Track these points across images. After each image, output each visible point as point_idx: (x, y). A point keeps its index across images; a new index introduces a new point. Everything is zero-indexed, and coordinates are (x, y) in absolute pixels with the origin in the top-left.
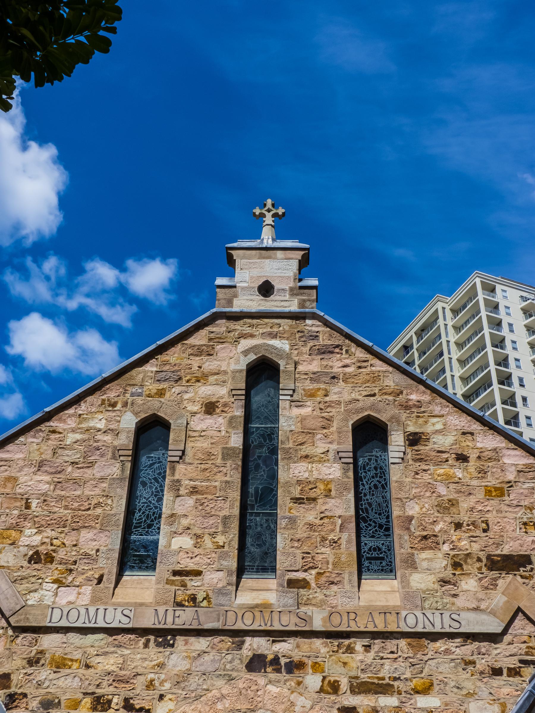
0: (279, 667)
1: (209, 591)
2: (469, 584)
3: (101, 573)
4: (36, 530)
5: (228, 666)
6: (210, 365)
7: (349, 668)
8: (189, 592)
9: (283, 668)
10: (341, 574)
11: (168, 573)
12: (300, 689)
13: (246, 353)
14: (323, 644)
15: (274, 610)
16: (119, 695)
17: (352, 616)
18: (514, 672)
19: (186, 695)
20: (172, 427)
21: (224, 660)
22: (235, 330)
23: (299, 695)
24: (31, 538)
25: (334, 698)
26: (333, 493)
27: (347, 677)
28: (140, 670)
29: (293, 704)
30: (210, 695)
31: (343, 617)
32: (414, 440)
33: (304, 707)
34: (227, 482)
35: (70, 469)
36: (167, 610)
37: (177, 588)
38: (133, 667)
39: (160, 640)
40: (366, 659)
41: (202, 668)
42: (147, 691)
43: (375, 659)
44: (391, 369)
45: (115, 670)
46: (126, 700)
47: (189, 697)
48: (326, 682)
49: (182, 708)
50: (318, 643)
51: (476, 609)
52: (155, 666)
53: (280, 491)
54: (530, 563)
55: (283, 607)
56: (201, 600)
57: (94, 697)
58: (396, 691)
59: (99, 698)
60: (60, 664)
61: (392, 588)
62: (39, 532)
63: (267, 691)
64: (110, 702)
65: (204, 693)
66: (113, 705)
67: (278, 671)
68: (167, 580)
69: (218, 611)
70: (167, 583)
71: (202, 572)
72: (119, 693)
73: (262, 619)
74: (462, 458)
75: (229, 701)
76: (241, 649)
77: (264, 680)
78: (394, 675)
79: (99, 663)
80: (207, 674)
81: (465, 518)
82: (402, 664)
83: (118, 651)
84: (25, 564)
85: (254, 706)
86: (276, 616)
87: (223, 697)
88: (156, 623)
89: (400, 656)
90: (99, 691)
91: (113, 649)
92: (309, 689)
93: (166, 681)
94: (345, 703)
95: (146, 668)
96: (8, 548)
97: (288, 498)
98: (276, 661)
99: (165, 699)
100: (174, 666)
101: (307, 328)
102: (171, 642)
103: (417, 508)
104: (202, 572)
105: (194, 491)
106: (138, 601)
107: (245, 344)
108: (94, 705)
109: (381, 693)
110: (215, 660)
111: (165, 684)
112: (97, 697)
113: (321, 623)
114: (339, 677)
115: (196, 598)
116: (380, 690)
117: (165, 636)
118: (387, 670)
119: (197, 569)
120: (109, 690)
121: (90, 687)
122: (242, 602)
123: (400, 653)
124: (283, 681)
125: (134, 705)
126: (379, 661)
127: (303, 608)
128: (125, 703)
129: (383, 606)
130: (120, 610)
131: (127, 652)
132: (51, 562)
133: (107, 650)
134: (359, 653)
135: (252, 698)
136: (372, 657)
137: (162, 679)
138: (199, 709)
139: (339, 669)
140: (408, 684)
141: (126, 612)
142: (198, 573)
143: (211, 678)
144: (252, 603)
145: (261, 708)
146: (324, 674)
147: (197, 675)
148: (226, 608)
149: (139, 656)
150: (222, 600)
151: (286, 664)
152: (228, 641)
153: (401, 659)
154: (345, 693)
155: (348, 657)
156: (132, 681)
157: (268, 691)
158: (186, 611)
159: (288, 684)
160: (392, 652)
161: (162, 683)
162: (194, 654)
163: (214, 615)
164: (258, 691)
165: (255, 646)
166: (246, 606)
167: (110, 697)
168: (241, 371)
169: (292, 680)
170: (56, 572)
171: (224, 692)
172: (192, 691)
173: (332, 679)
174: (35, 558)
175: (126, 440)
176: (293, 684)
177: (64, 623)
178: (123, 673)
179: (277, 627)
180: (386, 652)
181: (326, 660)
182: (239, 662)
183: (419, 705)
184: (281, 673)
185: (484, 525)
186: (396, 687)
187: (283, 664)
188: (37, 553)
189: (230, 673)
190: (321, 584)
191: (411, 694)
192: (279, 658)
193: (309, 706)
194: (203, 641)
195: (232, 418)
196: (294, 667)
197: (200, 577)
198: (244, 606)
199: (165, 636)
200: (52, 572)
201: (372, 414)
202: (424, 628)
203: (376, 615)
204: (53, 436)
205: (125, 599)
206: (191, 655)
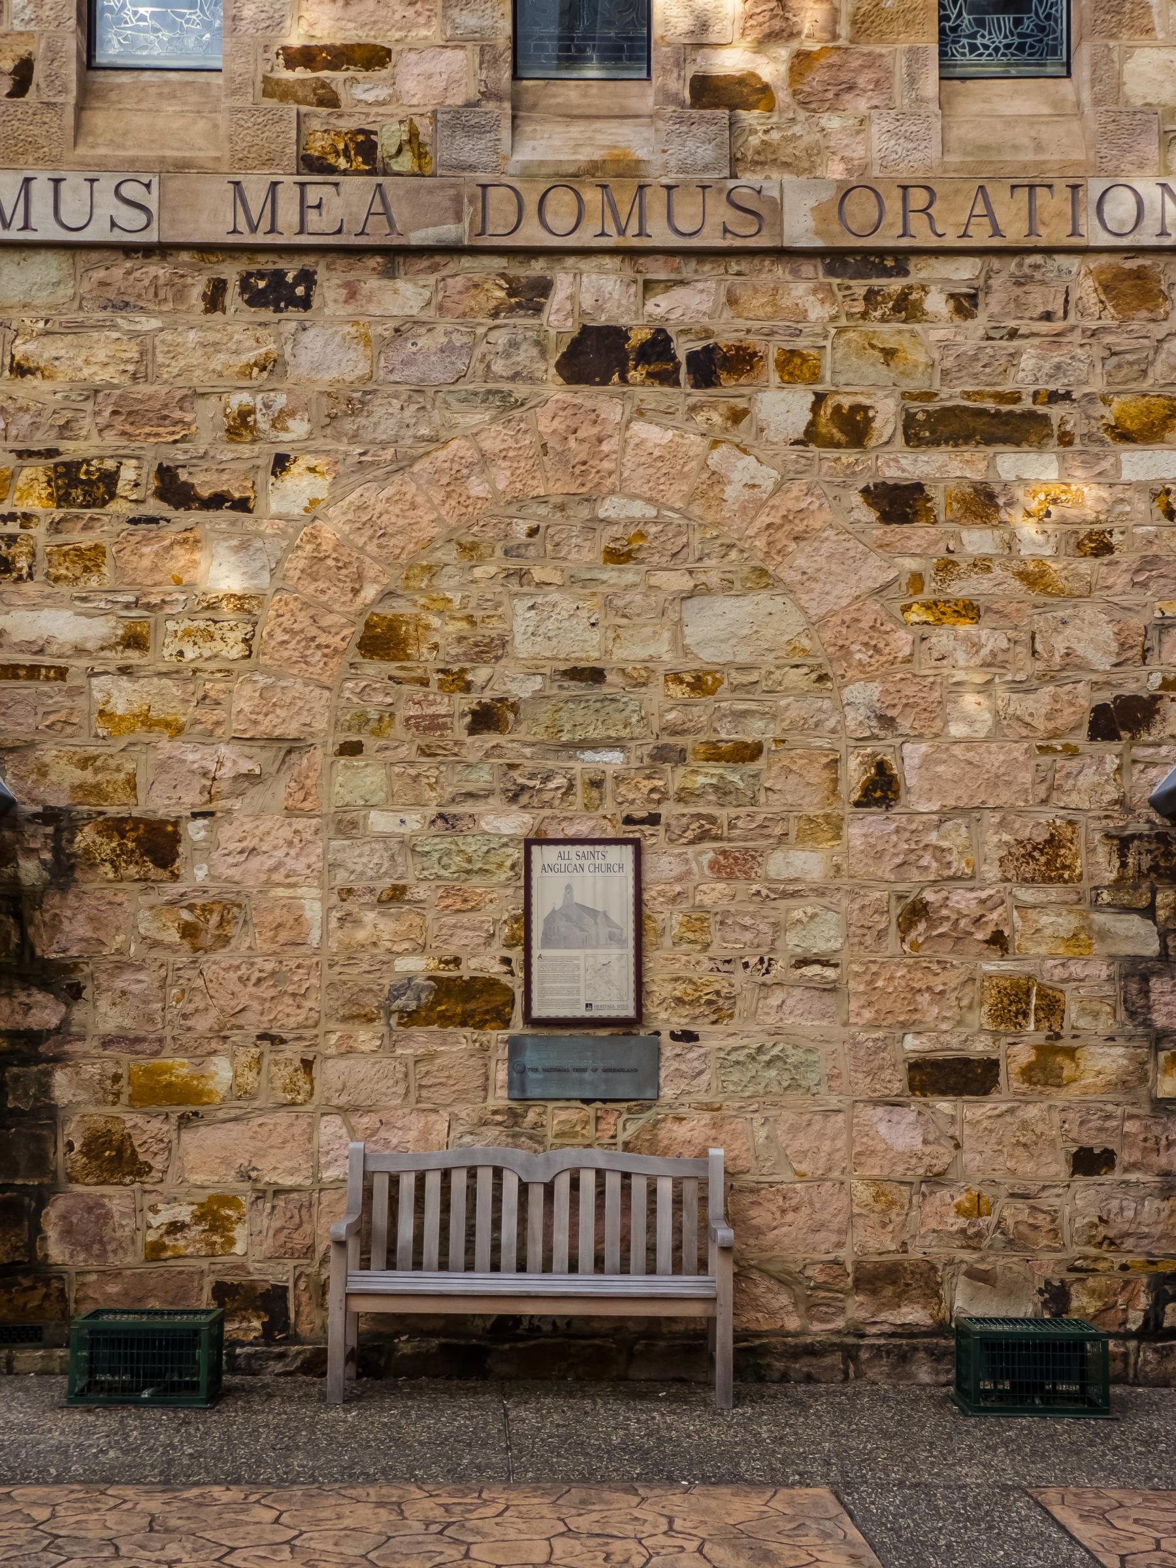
0: (670, 367)
1: (416, 120)
3: (22, 51)
5: (498, 367)
7: (901, 368)
8: (346, 124)
9: (683, 369)
10: (881, 55)
11: (267, 55)
12: (742, 433)
14: (815, 291)
15: (647, 181)
16: (138, 458)
17: (919, 198)
19: (361, 454)
21: (483, 348)
23: (737, 452)
25: (852, 459)
27: (897, 394)
28: (198, 379)
29: (717, 479)
30: (442, 454)
31: (887, 203)
33: (754, 486)
36: (274, 184)
37: (304, 109)
38: (176, 371)
39: (262, 284)
40: (960, 338)
41: (413, 373)
42: (233, 447)
43: (989, 338)
45: (115, 381)
46: (166, 474)
47: (372, 463)
48: (826, 411)
49: (354, 495)
52: (251, 367)
55: (681, 170)
56: (393, 150)
57: (56, 465)
58: (1056, 433)
61: (1055, 104)
63: (633, 442)
64: (110, 479)
65: (421, 451)
66: (122, 488)
67: (669, 378)
68: (266, 79)
69: (452, 186)
70: (266, 93)
71: (389, 52)
72: (137, 453)
73: (608, 210)
75: (508, 473)
76: (538, 310)
77: (619, 409)
78: (1052, 387)
79: (57, 359)
80: (430, 392)
82: (1079, 351)
83: (119, 321)
85: (589, 485)
86: (656, 202)
87: (485, 460)
88: (242, 226)
89: (1073, 329)
90: (72, 449)
91: (101, 315)
92: (770, 434)
93: (292, 414)
94: (888, 474)
95: (220, 375)
99: (296, 469)
100: (316, 367)
102: (300, 291)
104: (389, 52)
106: (168, 153)
108: (58, 488)
109: (1005, 441)
110: (454, 348)
111: (291, 423)
112: (64, 464)
113: (810, 223)
114: (869, 395)
115: (374, 145)
116: (1000, 431)
118: (1029, 370)
119: (372, 41)
120: (104, 443)
121: (38, 435)
122: (537, 157)
123: (1072, 319)
124: (683, 409)
125: (192, 486)
126: (1004, 343)
127: (748, 175)
128: (162, 480)
129: (1025, 166)
130: (107, 183)
131: (149, 324)
133: (81, 316)
134: (935, 320)
135: (584, 463)
136: (981, 332)
137: (277, 406)
138: (408, 497)
139: (875, 370)
140: (1097, 414)
141: (128, 190)
142: (375, 58)
143: (445, 402)
144: (573, 158)
145: (613, 492)
146: (819, 388)
147: (396, 396)
148: (484, 177)
149: (192, 336)
150: (468, 149)
151: (692, 357)
153: (1076, 337)
154: (887, 443)
155: (900, 332)
156: (177, 414)
157: (637, 440)
158: (342, 189)
159: (699, 419)
160: (1048, 316)
161: (279, 421)
162: (380, 329)
163: (443, 199)
164: (600, 441)
165: (587, 301)
166: (550, 170)
167: (110, 464)
169: (713, 406)
171: (490, 444)
172: (384, 445)
173: (847, 402)
176: (716, 418)
178: (144, 389)
179: (660, 235)
180: (1028, 314)
181: (828, 343)
182: (535, 352)
183: (1127, 475)
184: (677, 383)
186: (1055, 422)
187: (681, 357)
189: (506, 386)
190: (809, 94)
191: (1102, 442)
192: (669, 340)
193: (769, 485)
194: (410, 286)
197: (384, 73)
198: (544, 171)
202: (1163, 233)
203: (999, 195)
205: (123, 147)
206: (371, 332)
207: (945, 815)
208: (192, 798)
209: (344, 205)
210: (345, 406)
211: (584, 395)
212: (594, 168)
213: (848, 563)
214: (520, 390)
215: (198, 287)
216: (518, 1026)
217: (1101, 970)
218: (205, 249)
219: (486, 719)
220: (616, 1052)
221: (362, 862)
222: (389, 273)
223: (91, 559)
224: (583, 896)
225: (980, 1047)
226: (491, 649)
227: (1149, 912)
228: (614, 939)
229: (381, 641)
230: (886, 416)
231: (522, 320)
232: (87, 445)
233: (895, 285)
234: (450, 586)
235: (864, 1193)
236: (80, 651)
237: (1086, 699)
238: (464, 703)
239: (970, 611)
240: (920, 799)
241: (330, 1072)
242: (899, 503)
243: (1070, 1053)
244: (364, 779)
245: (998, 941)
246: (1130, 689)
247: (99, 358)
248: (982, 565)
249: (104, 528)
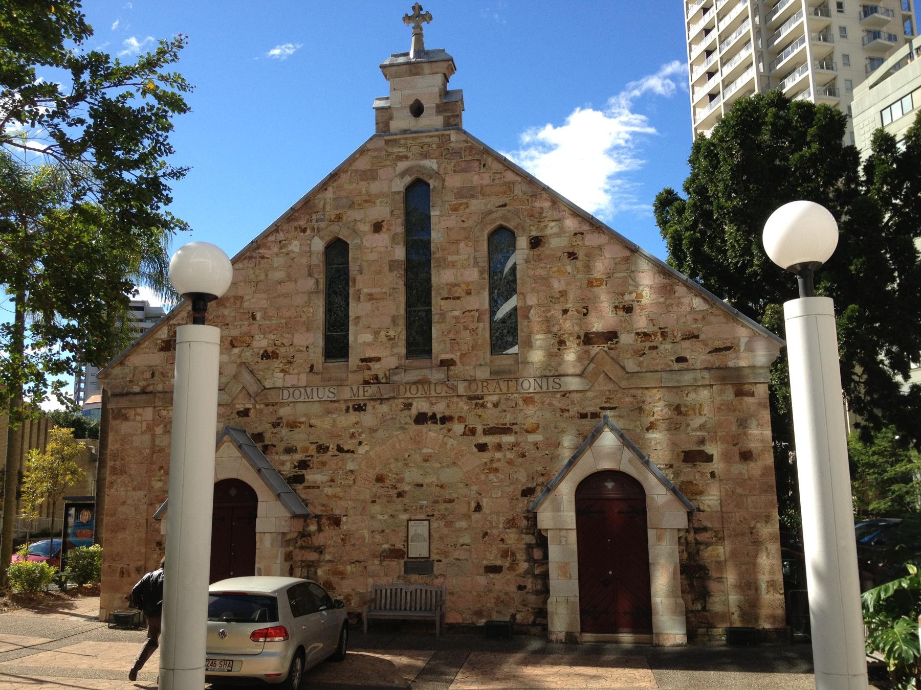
4: (262, 336)
6: (375, 187)
8: (373, 373)
12: (451, 434)
13: (402, 175)
17: (485, 384)
20: (350, 247)
22: (393, 153)
24: (261, 343)
26: (473, 292)
29: (446, 444)
32: (536, 242)
34: (394, 289)
35: (279, 287)
44: (519, 179)
46: (338, 446)
53: (433, 293)
54: (617, 337)
59: (320, 446)
60: (293, 425)
62: (265, 337)
64: (328, 447)
74: (572, 255)
84: (260, 360)
86: (432, 387)
96: (245, 349)
97: (439, 298)
98: (434, 415)
101: (452, 145)
103: (535, 299)
105: (371, 297)
107: (402, 166)
131: (334, 416)
132: (277, 358)
141: (332, 390)
142: (378, 359)
161: (360, 435)
168: (399, 193)
170: (281, 365)
174: (266, 355)
175: (318, 260)
177: (291, 399)
185: (585, 311)
188: (266, 351)
195: (395, 234)
200: (277, 364)
201: (503, 223)
204: (262, 261)
207: (491, 513)
208: (344, 513)
209: (372, 390)
210: (373, 431)
211: (419, 427)
212: (415, 383)
214: (407, 426)
215: (344, 408)
216: (406, 559)
217: (524, 546)
218: (345, 401)
219: (400, 495)
220: (423, 566)
221: (376, 525)
222: (381, 403)
223: (324, 464)
224: (419, 532)
225: (499, 563)
226: (401, 480)
227: (533, 534)
228: (425, 540)
229: (380, 479)
230: (480, 429)
231: (407, 412)
232: (324, 441)
233: (481, 401)
234: (392, 466)
235: (475, 594)
236: (322, 482)
237: (520, 488)
238: (395, 491)
239: (496, 470)
240: (486, 509)
241: (370, 568)
242: (482, 448)
243: (517, 564)
244: (376, 508)
245: (502, 540)
246: (530, 486)
247: (325, 424)
248: (499, 460)
249: (326, 457)
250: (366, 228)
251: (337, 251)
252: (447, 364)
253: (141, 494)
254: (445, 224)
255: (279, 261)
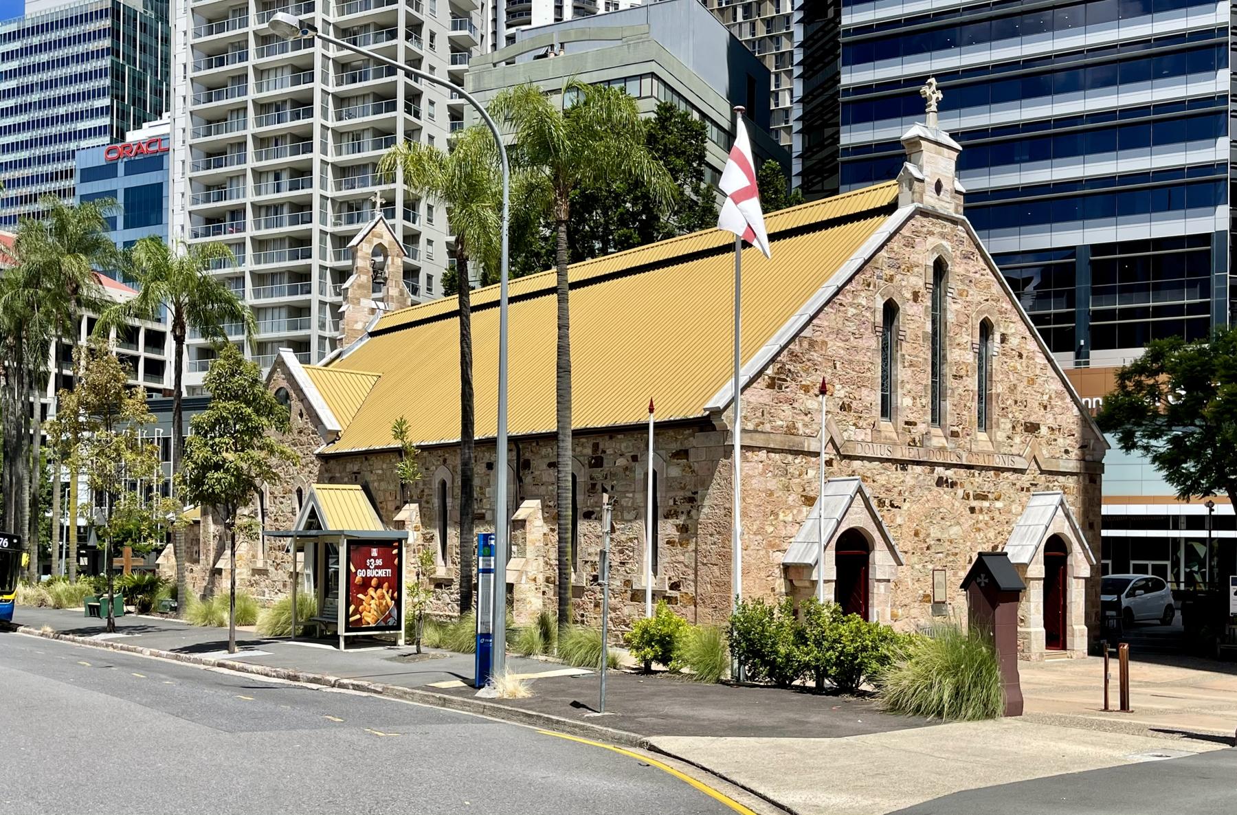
2: (1017, 439)
18: (1028, 490)
32: (1004, 339)
50: (962, 471)
51: (1019, 455)
81: (1019, 399)
107: (932, 241)
117: (903, 464)
152: (927, 469)
196: (953, 484)
199: (903, 464)
213: (968, 520)
219: (928, 548)
226: (928, 535)
239: (979, 530)
244: (915, 559)
249: (885, 513)
250: (909, 295)
251: (891, 310)
252: (954, 434)
253: (759, 537)
254: (955, 307)
255: (851, 311)
